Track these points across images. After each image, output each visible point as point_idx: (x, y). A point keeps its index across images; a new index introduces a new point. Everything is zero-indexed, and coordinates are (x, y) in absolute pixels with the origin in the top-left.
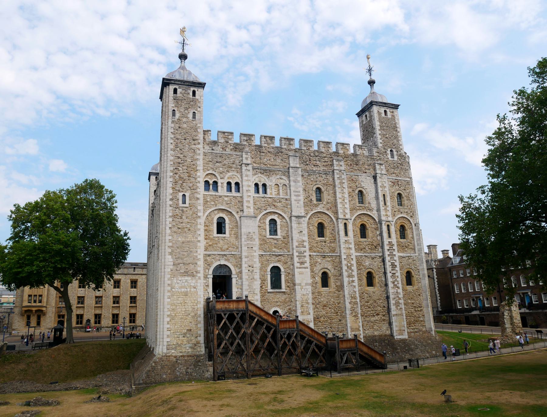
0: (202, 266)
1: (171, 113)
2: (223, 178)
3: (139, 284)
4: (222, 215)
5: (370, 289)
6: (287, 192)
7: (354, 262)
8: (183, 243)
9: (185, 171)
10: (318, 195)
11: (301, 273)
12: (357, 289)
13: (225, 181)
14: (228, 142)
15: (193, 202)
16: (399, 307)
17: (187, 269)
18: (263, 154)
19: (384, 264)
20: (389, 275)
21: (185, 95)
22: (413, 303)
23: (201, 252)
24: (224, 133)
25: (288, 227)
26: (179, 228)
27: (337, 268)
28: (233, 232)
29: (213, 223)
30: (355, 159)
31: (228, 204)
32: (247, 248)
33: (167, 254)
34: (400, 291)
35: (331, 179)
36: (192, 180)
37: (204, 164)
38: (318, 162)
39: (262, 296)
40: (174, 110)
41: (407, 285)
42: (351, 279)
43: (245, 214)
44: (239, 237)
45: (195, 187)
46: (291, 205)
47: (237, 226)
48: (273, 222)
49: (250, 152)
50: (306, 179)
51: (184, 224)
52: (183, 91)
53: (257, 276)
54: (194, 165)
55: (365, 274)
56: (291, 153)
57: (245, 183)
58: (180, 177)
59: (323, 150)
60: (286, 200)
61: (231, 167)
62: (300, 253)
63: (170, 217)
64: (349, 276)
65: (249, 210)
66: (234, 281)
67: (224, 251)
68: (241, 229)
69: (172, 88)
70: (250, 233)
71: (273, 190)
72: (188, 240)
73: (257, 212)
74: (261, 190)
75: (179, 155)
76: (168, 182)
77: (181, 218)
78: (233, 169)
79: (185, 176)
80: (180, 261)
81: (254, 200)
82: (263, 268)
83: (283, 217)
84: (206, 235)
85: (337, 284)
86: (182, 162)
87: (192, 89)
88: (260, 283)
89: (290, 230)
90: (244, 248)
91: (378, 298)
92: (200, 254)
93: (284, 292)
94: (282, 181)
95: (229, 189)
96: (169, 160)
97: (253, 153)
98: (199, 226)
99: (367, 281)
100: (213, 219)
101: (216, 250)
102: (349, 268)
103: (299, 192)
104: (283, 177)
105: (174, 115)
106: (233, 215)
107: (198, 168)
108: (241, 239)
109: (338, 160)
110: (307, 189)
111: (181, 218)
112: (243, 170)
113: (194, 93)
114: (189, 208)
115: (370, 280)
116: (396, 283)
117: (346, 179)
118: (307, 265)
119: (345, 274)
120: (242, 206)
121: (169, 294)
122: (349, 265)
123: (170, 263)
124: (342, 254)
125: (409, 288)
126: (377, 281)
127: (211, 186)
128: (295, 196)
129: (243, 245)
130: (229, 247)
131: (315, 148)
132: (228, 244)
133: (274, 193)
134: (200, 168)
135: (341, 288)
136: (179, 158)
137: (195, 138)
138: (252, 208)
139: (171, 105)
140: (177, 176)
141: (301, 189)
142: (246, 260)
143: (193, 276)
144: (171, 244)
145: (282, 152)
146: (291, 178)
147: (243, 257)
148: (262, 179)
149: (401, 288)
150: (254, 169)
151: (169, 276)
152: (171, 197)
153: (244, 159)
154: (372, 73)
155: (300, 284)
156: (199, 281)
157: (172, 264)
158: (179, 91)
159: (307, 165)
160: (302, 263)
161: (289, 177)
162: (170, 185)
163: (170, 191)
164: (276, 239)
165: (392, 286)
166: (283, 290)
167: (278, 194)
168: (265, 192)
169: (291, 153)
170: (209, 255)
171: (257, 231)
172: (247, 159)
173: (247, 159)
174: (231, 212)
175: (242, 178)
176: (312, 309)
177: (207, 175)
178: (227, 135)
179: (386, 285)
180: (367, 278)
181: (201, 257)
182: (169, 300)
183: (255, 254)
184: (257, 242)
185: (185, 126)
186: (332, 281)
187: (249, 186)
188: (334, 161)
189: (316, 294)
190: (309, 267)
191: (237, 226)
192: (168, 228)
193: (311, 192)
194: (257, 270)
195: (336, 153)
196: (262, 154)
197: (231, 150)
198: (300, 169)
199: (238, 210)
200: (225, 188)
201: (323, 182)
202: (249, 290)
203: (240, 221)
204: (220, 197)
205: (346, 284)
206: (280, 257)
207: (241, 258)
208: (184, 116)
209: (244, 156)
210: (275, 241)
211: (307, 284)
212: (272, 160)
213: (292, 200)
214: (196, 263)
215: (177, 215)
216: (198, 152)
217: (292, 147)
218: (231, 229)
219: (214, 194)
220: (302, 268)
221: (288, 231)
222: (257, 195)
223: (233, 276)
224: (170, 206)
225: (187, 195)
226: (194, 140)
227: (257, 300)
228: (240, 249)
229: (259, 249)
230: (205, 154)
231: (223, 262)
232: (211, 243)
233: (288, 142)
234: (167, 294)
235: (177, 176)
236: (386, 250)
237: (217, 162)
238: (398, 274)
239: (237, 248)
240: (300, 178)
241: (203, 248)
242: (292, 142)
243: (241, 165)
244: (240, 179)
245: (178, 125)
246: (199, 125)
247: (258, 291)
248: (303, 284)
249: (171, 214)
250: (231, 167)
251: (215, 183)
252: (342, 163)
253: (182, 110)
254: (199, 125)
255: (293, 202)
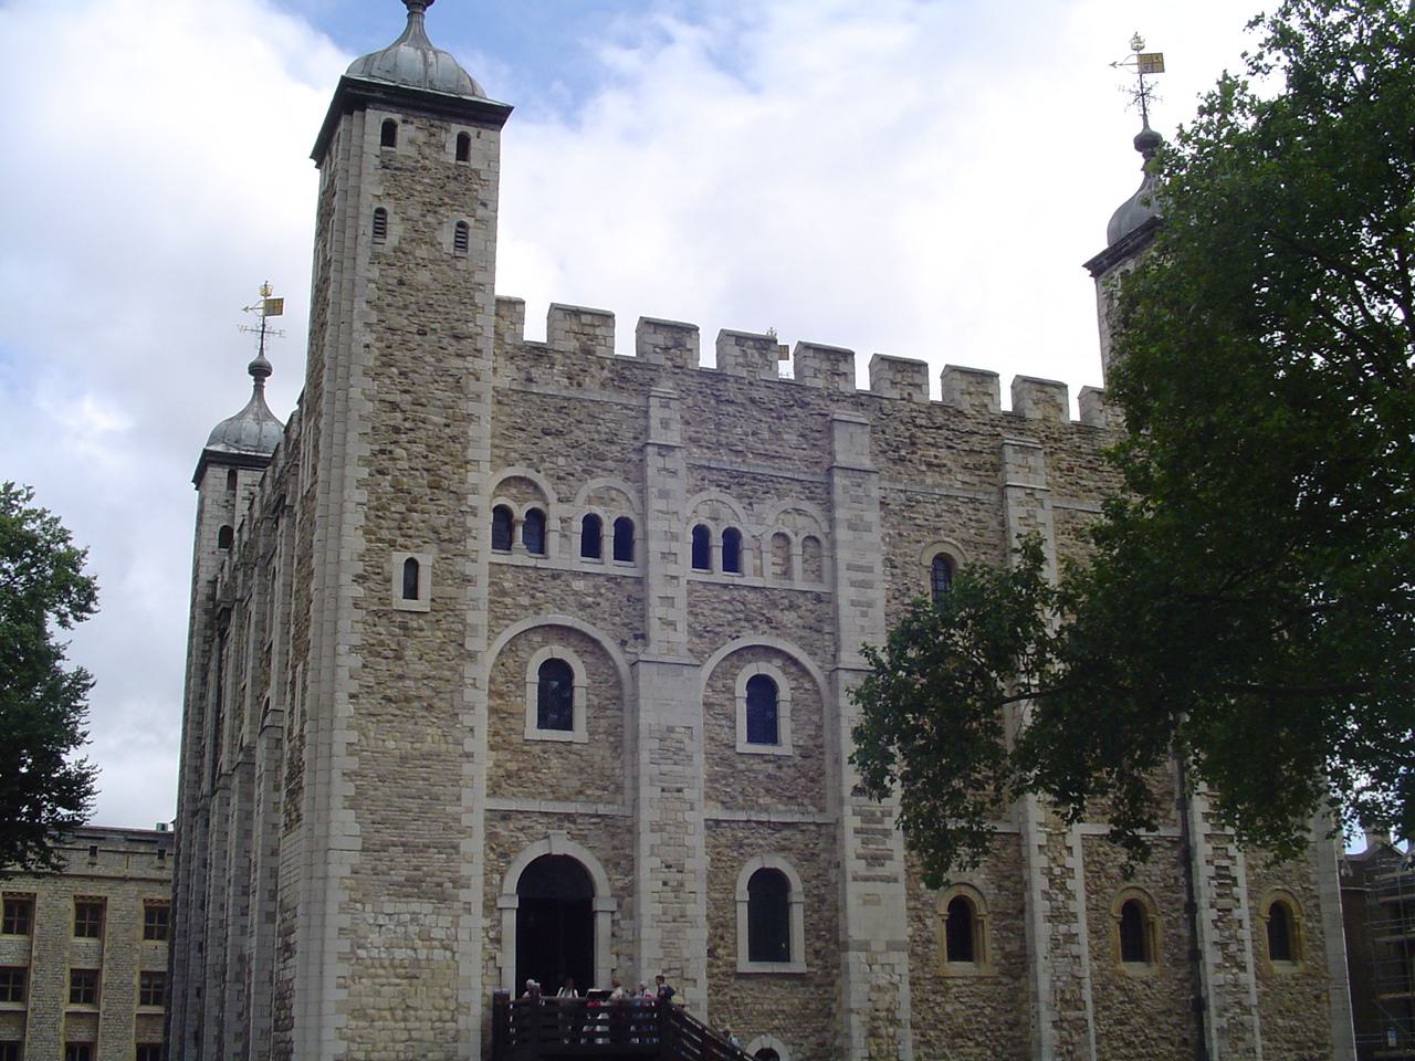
0: (479, 859)
1: (366, 224)
2: (568, 500)
3: (111, 918)
4: (559, 651)
5: (1135, 969)
6: (819, 569)
7: (1076, 862)
8: (404, 759)
9: (418, 463)
10: (941, 585)
11: (870, 900)
12: (1087, 968)
13: (577, 512)
14: (587, 351)
15: (450, 591)
16: (1241, 1045)
17: (417, 868)
18: (730, 409)
19: (1189, 874)
20: (1207, 915)
21: (427, 151)
22: (1293, 1031)
23: (476, 802)
24: (576, 313)
25: (820, 710)
26: (389, 699)
27: (1007, 884)
28: (603, 722)
29: (521, 685)
30: (1085, 448)
31: (584, 607)
32: (657, 792)
33: (337, 802)
34: (1248, 978)
35: (994, 524)
36: (446, 501)
37: (493, 436)
38: (943, 452)
39: (715, 989)
40: (380, 211)
41: (1273, 957)
42: (1063, 928)
43: (654, 650)
44: (628, 743)
45: (455, 532)
46: (835, 620)
47: (620, 698)
48: (762, 690)
49: (680, 398)
50: (894, 520)
51: (408, 683)
52: (421, 137)
53: (698, 908)
54: (453, 438)
55: (1115, 908)
56: (841, 412)
57: (656, 525)
58: (397, 488)
59: (965, 404)
60: (818, 598)
61: (601, 457)
62: (869, 817)
63: (354, 649)
64: (1054, 917)
65: (670, 630)
66: (603, 925)
67: (566, 799)
68: (635, 711)
69: (375, 118)
70: (671, 730)
71: (768, 558)
72: (426, 747)
73: (701, 645)
74: (717, 556)
75: (397, 398)
76: (350, 506)
77: (399, 658)
78: (610, 464)
79: (419, 485)
80: (388, 835)
81: (690, 593)
82: (718, 875)
83: (805, 672)
84: (496, 733)
85: (1008, 948)
86: (407, 425)
87: (456, 129)
88: (706, 935)
89: (827, 721)
90: (648, 792)
91: (1162, 1007)
92: (470, 810)
93: (799, 977)
94: (801, 521)
95: (591, 546)
96: (354, 415)
97: (690, 401)
98: (469, 695)
99: (1124, 937)
100: (523, 665)
101: (533, 796)
102: (1058, 882)
103: (870, 570)
104: (806, 505)
105: (380, 227)
106: (605, 655)
107: (471, 454)
108: (635, 752)
109: (1024, 449)
110: (898, 561)
111: (399, 658)
112: (651, 471)
113: (463, 144)
114: (429, 617)
115: (1134, 933)
116: (1233, 948)
117: (1050, 523)
118: (896, 866)
119: (1041, 907)
120: (643, 617)
121: (344, 969)
122: (1057, 871)
123: (347, 843)
124: (1033, 827)
125: (1281, 968)
126: (1160, 936)
127: (519, 531)
128: (853, 584)
129: (644, 780)
130: (583, 784)
131: (935, 393)
132: (582, 771)
133: (769, 570)
134: (481, 451)
135: (1019, 964)
136: (394, 406)
137: (461, 328)
138: (682, 626)
139: (372, 189)
140: (386, 482)
141: (876, 560)
142: (656, 838)
143: (443, 898)
144: (353, 764)
145: (804, 405)
146: (841, 514)
147: (644, 827)
148: (724, 511)
149: (1251, 968)
150: (693, 467)
151: (344, 896)
152: (359, 568)
153: (654, 423)
154: (1152, 106)
155: (864, 946)
156: (464, 920)
157: (358, 844)
158: (404, 132)
159: (902, 459)
160: (875, 860)
161: (829, 506)
162: (355, 518)
163: (355, 542)
164: (777, 760)
165: (1219, 960)
166: (798, 964)
167: (787, 573)
168: (732, 562)
169: (841, 412)
170: (506, 816)
171: (698, 719)
172: (665, 424)
173: (665, 424)
174: (595, 642)
175: (643, 502)
176: (909, 1044)
177: (506, 482)
178: (582, 326)
179: (1196, 955)
180: (1123, 926)
181: (477, 822)
182: (342, 994)
183: (689, 816)
184: (699, 768)
185: (423, 277)
186: (988, 937)
187: (674, 537)
188: (1009, 451)
189: (927, 986)
190: (902, 877)
191: (618, 698)
192: (342, 697)
193: (913, 572)
194: (697, 885)
195: (1016, 418)
196: (722, 407)
197: (603, 385)
198: (874, 476)
199: (626, 634)
200: (577, 541)
201: (961, 533)
202: (664, 965)
203: (635, 678)
204: (556, 576)
205: (1042, 947)
206: (787, 833)
207: (632, 830)
208: (418, 236)
209: (656, 413)
210: (770, 768)
211: (892, 946)
212: (766, 435)
213: (843, 602)
214: (455, 847)
215: (382, 643)
216: (473, 386)
217: (843, 386)
218: (598, 711)
219: (532, 562)
220: (873, 879)
221: (820, 727)
222: (701, 576)
223: (598, 905)
224: (356, 605)
225: (426, 561)
226: (457, 337)
227: (695, 1005)
228: (628, 793)
229: (708, 797)
230: (500, 398)
231: (562, 845)
232: (513, 766)
233: (826, 366)
234: (335, 970)
235: (386, 482)
236: (1198, 818)
237: (546, 432)
238: (1242, 912)
239: (619, 789)
240: (873, 515)
241: (482, 785)
242: (843, 367)
243: (641, 450)
244: (638, 508)
245: (395, 272)
246: (479, 277)
247: (699, 967)
248: (878, 946)
249: (356, 640)
250: (601, 457)
251: (537, 519)
252: (1037, 461)
253: (414, 213)
254: (479, 277)
255: (846, 610)
